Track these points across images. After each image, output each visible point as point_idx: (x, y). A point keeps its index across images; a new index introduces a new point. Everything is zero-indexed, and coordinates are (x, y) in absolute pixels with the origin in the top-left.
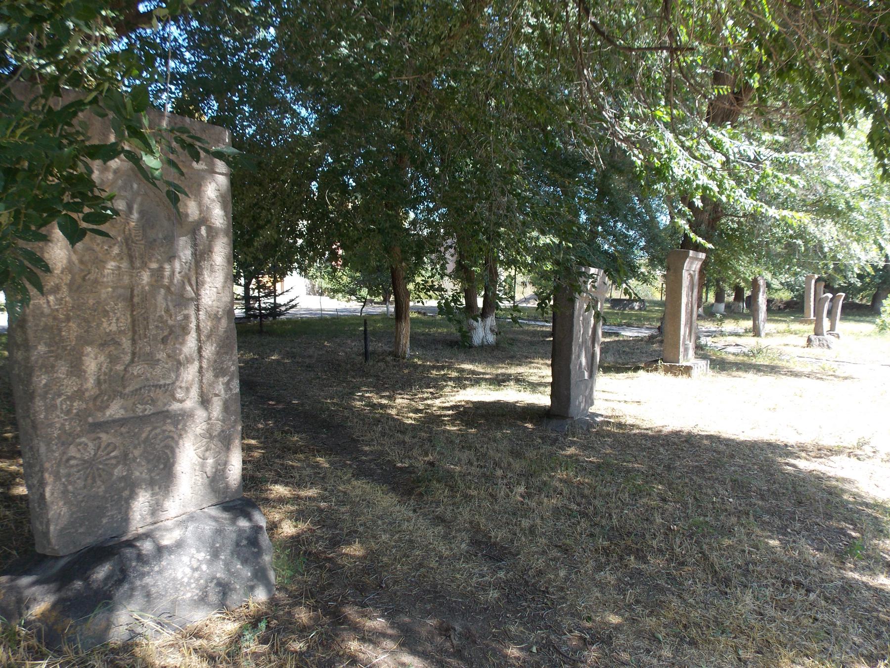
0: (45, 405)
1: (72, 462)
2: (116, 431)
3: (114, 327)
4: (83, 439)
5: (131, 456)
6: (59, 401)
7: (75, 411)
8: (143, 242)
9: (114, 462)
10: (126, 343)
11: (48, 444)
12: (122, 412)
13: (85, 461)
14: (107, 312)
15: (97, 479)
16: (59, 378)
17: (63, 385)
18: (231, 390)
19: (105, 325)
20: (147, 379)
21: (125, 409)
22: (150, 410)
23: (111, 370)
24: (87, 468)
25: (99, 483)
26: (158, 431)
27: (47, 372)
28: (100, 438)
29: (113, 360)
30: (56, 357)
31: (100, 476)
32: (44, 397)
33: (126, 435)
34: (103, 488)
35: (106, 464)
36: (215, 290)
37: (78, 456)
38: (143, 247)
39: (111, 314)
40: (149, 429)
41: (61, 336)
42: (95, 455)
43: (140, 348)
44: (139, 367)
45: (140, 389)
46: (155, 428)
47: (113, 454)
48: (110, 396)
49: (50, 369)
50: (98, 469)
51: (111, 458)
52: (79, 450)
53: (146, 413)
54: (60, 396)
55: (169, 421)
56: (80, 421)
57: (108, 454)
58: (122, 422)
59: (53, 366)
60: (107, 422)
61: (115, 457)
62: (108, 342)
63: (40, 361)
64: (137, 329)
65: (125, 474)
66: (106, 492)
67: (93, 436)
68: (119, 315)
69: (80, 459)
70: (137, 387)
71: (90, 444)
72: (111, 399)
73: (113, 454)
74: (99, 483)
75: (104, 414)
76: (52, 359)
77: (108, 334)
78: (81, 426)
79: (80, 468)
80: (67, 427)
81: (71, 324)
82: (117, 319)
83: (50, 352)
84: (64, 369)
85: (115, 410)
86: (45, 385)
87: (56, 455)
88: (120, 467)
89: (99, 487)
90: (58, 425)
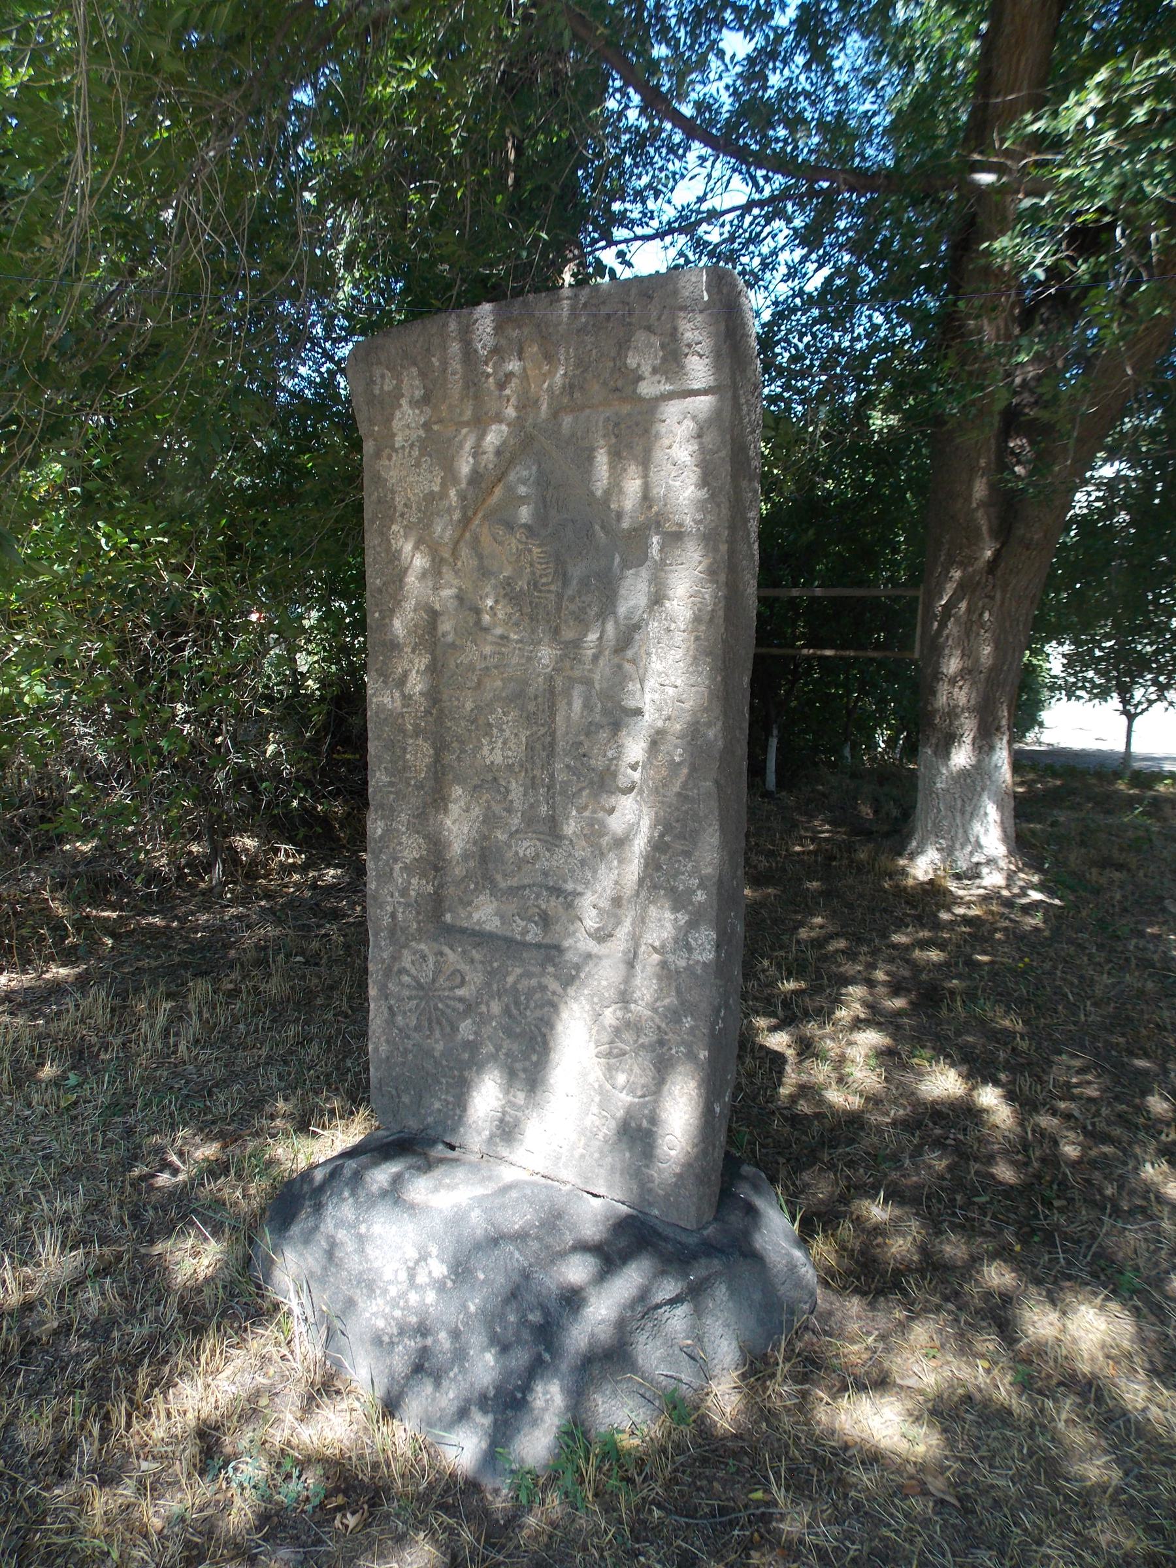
0: (376, 869)
1: (406, 979)
2: (464, 952)
3: (499, 760)
4: (423, 946)
5: (484, 1008)
6: (397, 867)
7: (413, 893)
8: (553, 588)
9: (461, 1007)
10: (516, 792)
11: (376, 935)
12: (497, 922)
13: (420, 986)
14: (489, 725)
15: (434, 1025)
16: (397, 830)
17: (401, 844)
18: (690, 949)
19: (486, 750)
20: (546, 874)
21: (502, 917)
22: (534, 934)
23: (485, 838)
24: (421, 999)
25: (437, 1034)
26: (534, 982)
27: (383, 818)
28: (441, 954)
29: (490, 819)
30: (396, 793)
31: (439, 1023)
32: (377, 858)
33: (480, 967)
34: (440, 1047)
35: (448, 1006)
36: (671, 691)
37: (413, 971)
38: (552, 596)
39: (495, 731)
40: (519, 971)
41: (405, 761)
42: (434, 980)
43: (532, 806)
44: (526, 844)
45: (524, 887)
46: (528, 975)
47: (460, 992)
48: (477, 884)
49: (389, 813)
50: (436, 1008)
51: (454, 999)
52: (413, 962)
53: (529, 938)
54: (396, 860)
55: (551, 969)
56: (418, 913)
57: (452, 989)
58: (480, 938)
59: (392, 810)
60: (463, 931)
61: (461, 1000)
62: (488, 782)
63: (378, 797)
64: (529, 766)
65: (471, 1038)
66: (443, 1054)
67: (436, 946)
68: (508, 733)
69: (414, 978)
70: (526, 882)
71: (431, 960)
72: (478, 890)
73: (460, 992)
74: (437, 1034)
75: (470, 916)
76: (392, 797)
77: (490, 768)
78: (419, 923)
79: (414, 993)
80: (400, 917)
81: (420, 741)
82: (504, 743)
83: (391, 784)
84: (404, 817)
85: (485, 913)
86: (381, 837)
87: (385, 955)
88: (469, 1021)
89: (437, 1041)
90: (389, 909)
